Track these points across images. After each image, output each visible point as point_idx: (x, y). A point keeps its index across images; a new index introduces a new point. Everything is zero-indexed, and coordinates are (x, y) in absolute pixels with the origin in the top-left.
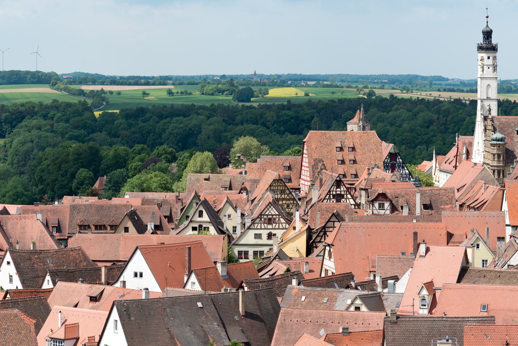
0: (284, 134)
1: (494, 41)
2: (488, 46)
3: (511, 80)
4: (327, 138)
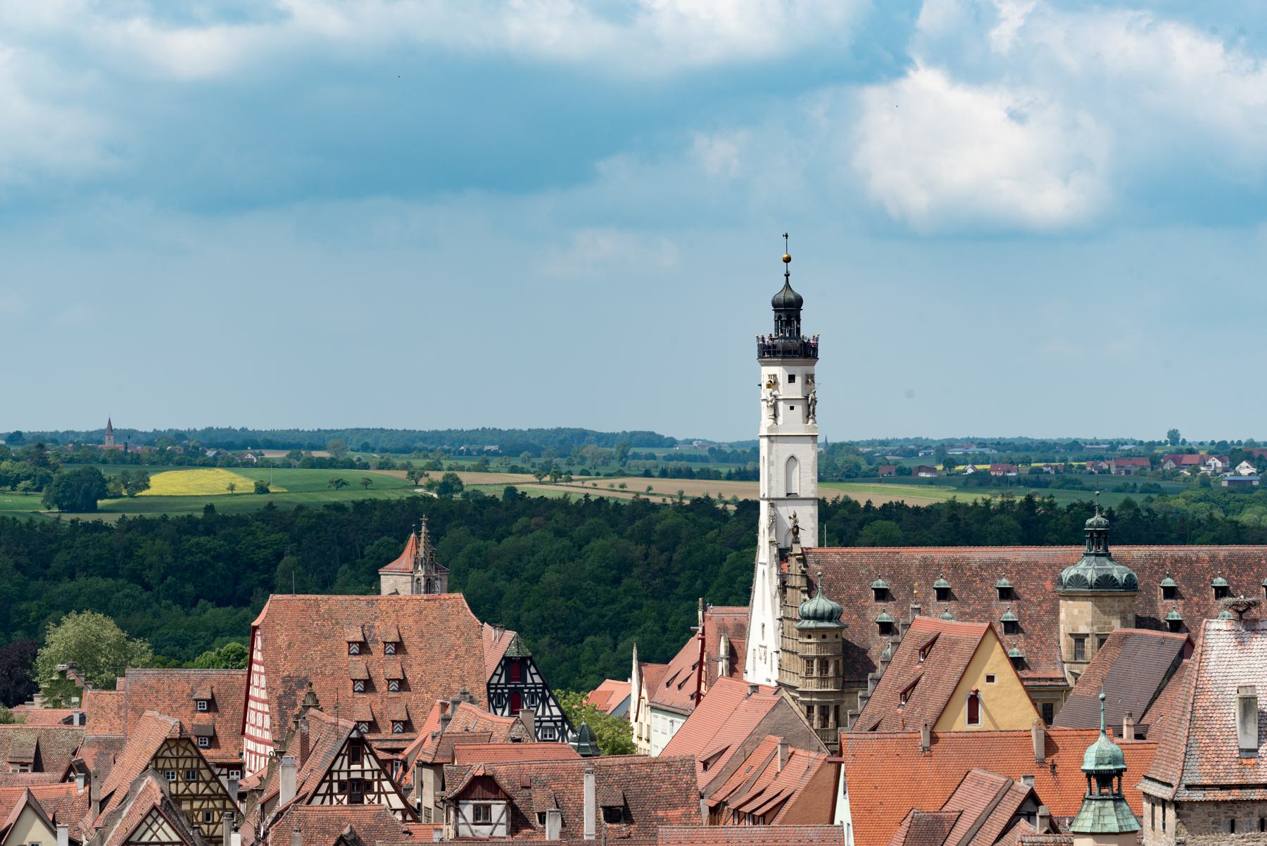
0: (194, 605)
1: (808, 328)
2: (790, 344)
3: (858, 443)
4: (321, 617)
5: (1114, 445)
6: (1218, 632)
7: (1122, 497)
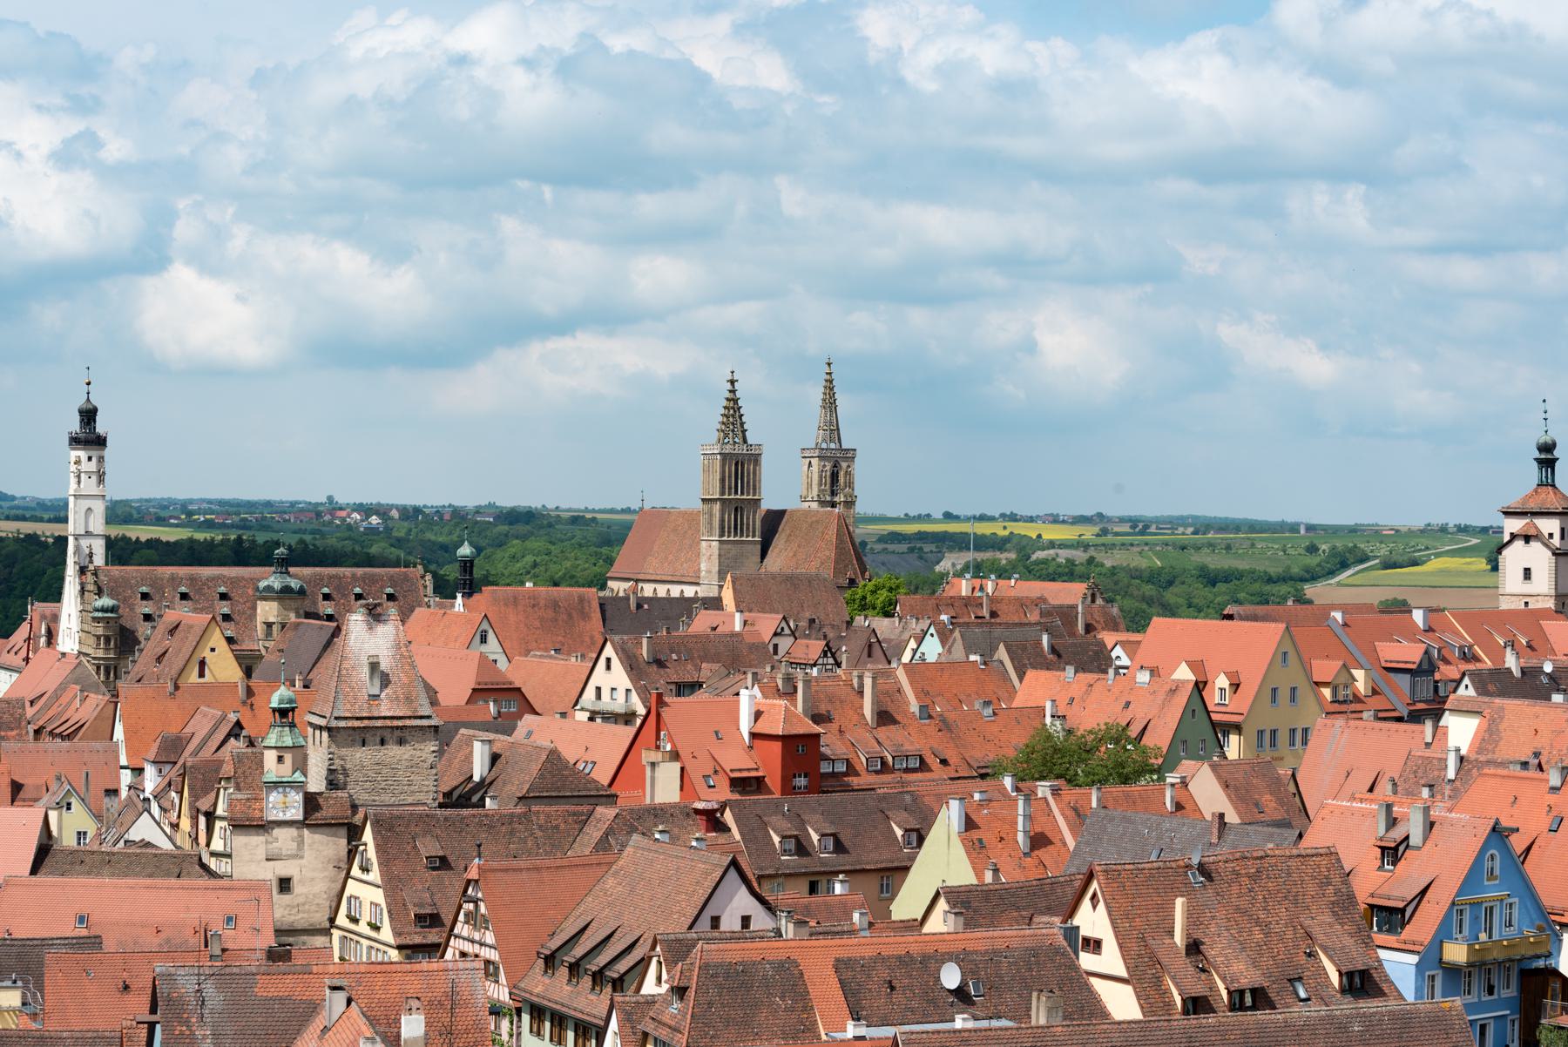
1: (101, 427)
2: (89, 438)
5: (293, 504)
6: (356, 622)
7: (297, 537)
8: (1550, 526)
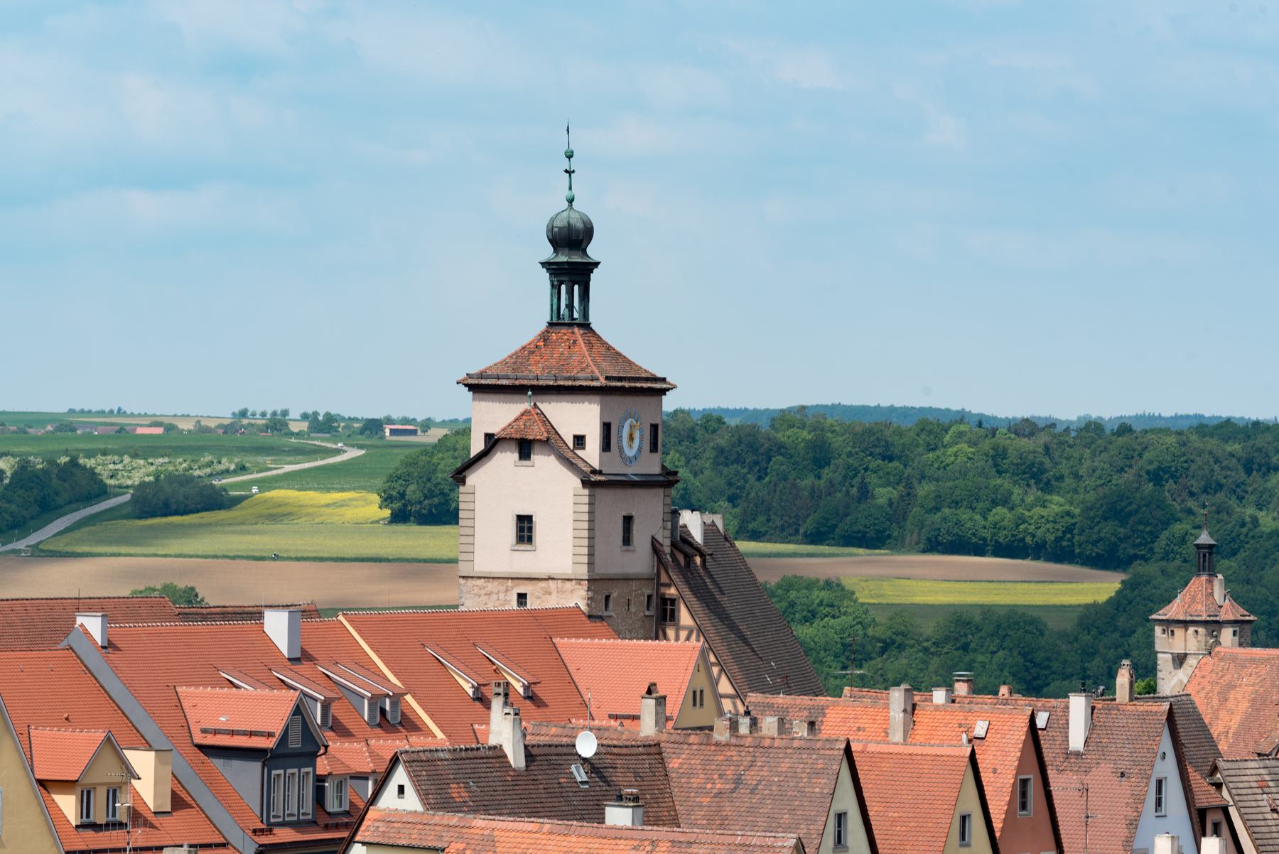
8: (578, 418)
